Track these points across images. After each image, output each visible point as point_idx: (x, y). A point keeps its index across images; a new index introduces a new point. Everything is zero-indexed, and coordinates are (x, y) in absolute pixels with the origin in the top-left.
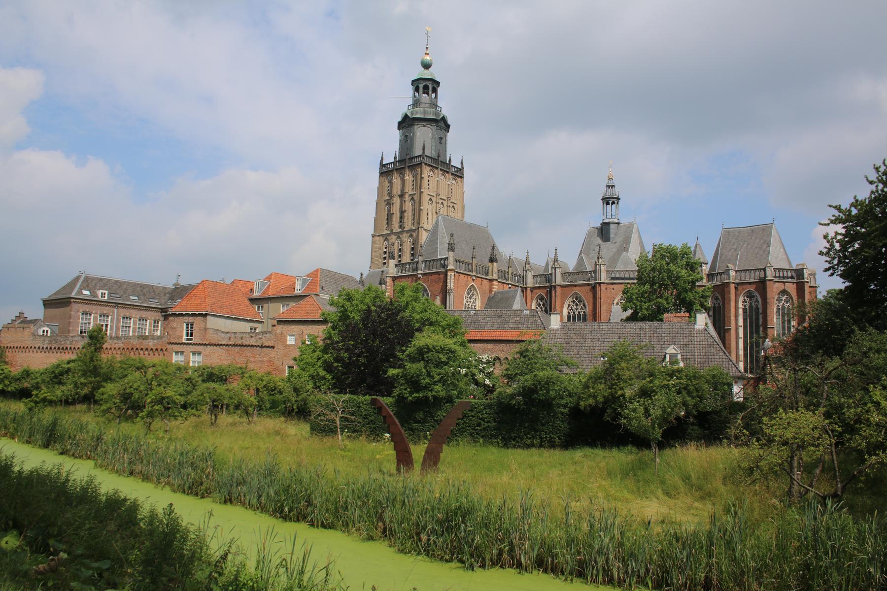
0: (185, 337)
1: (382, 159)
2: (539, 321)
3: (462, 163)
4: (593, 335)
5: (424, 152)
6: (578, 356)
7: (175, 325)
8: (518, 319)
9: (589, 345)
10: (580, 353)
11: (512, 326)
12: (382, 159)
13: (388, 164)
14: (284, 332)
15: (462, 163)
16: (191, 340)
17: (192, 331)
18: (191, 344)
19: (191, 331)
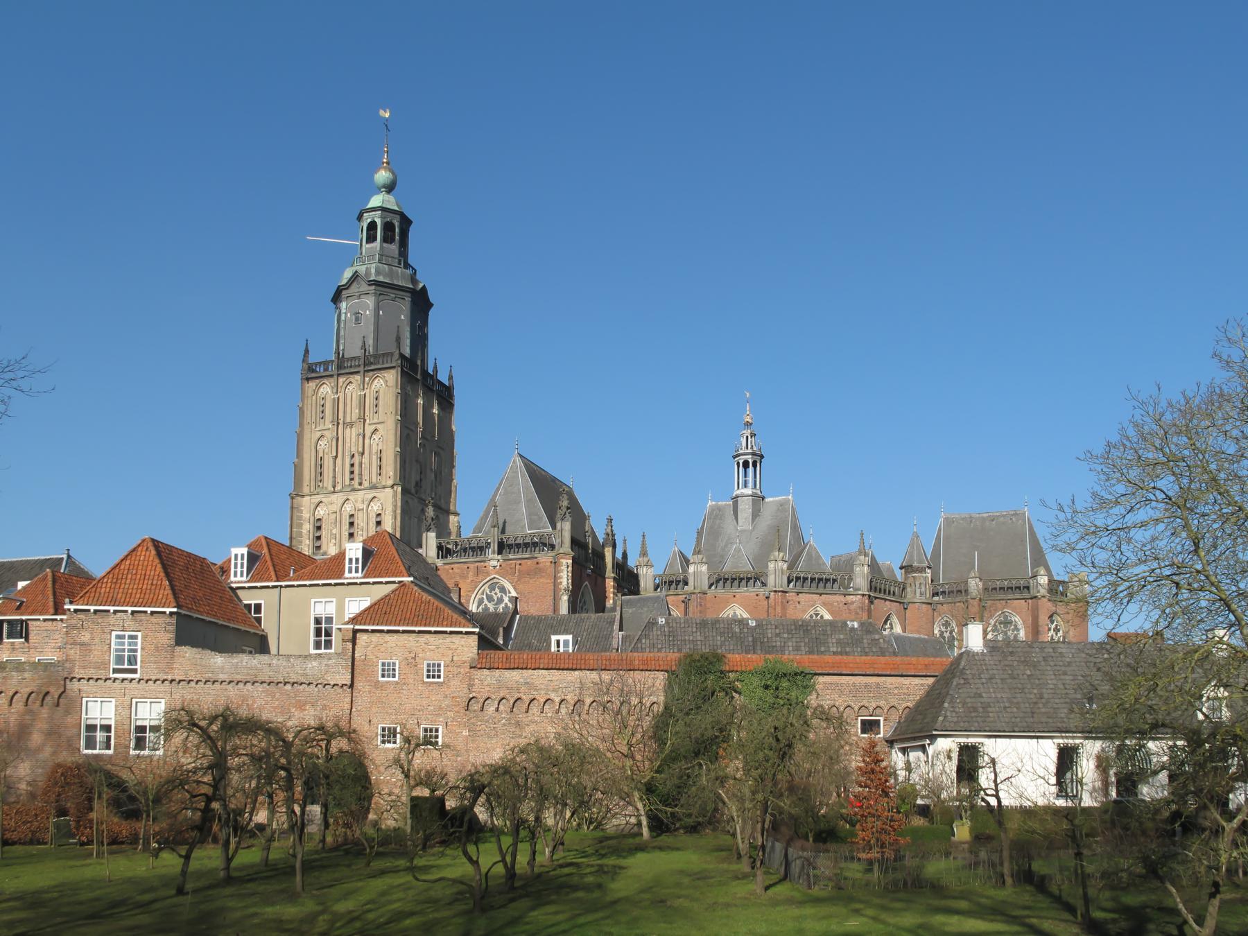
0: (113, 666)
1: (307, 351)
2: (881, 641)
3: (451, 378)
4: (1052, 664)
5: (399, 347)
6: (1043, 701)
7: (86, 637)
8: (842, 637)
9: (1055, 682)
10: (1046, 696)
11: (835, 649)
12: (307, 351)
13: (316, 364)
14: (371, 656)
15: (451, 378)
16: (135, 671)
17: (136, 651)
18: (132, 680)
19: (130, 651)
